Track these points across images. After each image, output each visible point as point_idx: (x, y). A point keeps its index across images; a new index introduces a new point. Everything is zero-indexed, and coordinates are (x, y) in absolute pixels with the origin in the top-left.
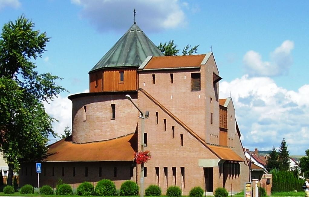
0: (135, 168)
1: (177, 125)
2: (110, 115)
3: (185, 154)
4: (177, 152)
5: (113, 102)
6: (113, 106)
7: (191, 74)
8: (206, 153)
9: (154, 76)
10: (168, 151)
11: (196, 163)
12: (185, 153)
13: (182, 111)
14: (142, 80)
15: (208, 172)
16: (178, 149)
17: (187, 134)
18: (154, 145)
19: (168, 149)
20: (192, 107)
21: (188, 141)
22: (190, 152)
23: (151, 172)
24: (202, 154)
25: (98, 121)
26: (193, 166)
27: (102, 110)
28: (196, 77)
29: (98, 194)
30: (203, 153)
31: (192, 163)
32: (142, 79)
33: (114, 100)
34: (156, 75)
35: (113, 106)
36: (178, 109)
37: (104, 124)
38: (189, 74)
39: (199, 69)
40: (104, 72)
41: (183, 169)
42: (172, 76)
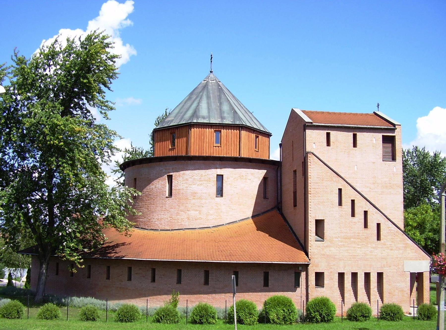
0: (303, 274)
1: (371, 210)
2: (213, 189)
3: (383, 252)
4: (372, 249)
5: (220, 171)
6: (220, 178)
7: (383, 136)
8: (414, 251)
9: (328, 135)
10: (358, 248)
11: (400, 266)
12: (384, 251)
13: (370, 188)
14: (312, 139)
15: (417, 278)
16: (374, 245)
17: (387, 223)
18: (336, 238)
19: (358, 245)
20: (386, 184)
21: (388, 233)
22: (392, 250)
23: (332, 279)
24: (409, 253)
25: (194, 199)
26: (395, 271)
27: (201, 182)
28: (389, 141)
29: (273, 320)
30: (410, 252)
31: (394, 265)
32: (311, 137)
33: (221, 168)
34: (333, 133)
35: (220, 178)
36: (366, 186)
37: (206, 203)
38: (379, 136)
39: (393, 130)
40: (192, 129)
41: (380, 275)
42: (355, 136)
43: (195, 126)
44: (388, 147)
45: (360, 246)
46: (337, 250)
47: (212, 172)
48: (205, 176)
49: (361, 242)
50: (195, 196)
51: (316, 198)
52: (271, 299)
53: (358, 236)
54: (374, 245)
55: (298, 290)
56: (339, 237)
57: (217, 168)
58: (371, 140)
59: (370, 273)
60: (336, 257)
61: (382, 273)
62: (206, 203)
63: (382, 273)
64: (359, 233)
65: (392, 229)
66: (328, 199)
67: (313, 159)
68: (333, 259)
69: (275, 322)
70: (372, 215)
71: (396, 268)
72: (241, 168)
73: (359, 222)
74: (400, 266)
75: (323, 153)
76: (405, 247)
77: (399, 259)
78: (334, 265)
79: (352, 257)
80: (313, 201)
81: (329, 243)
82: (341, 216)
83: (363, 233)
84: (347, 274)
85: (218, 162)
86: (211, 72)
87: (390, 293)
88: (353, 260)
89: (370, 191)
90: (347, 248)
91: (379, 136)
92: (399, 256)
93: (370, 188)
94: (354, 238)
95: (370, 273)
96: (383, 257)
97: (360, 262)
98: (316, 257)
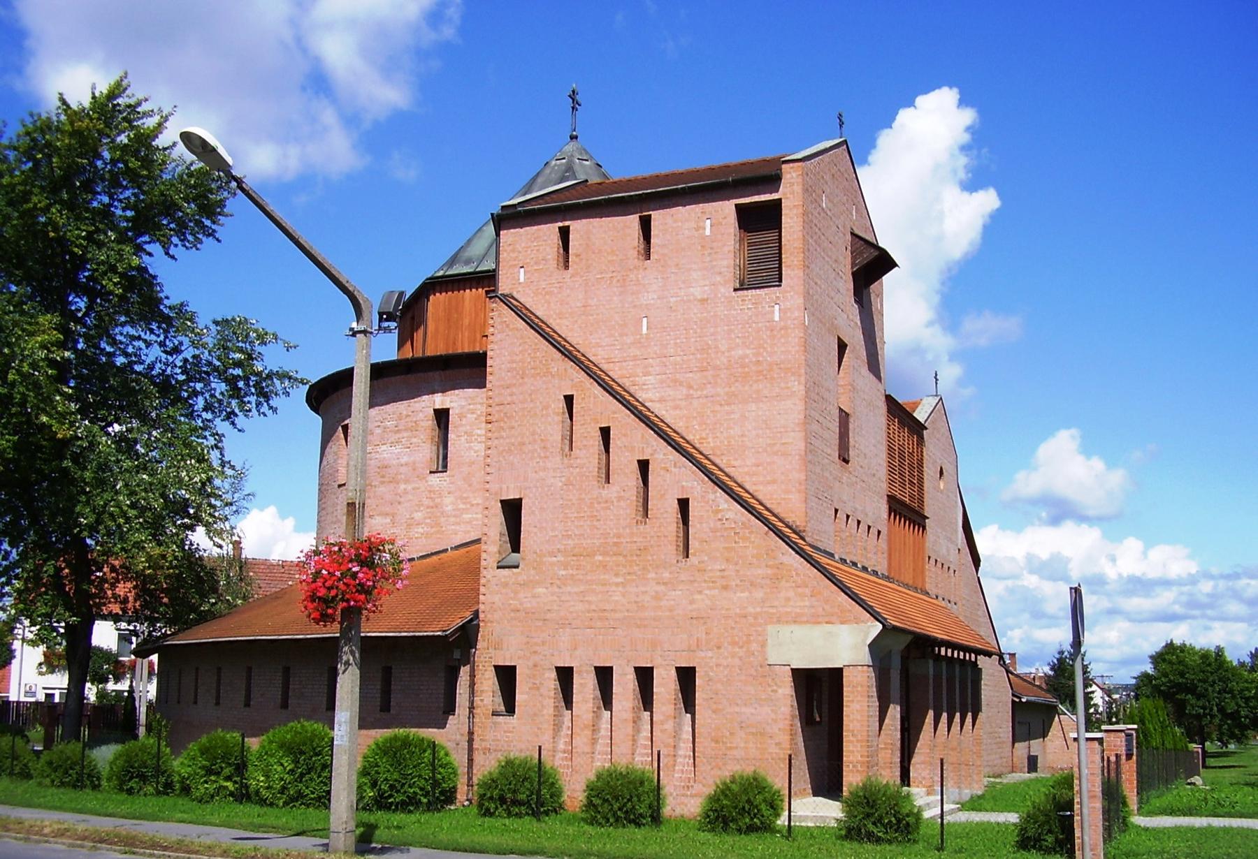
0: (464, 671)
1: (660, 454)
2: (426, 452)
3: (697, 597)
4: (662, 588)
5: (439, 400)
6: (442, 417)
7: (739, 207)
8: (807, 591)
9: (565, 233)
10: (617, 584)
11: (754, 646)
12: (700, 592)
13: (690, 387)
14: (513, 255)
15: (818, 691)
16: (666, 575)
17: (712, 496)
18: (552, 554)
19: (617, 575)
20: (743, 366)
21: (714, 531)
22: (725, 588)
23: (538, 689)
24: (788, 599)
25: (383, 483)
26: (737, 661)
27: (398, 436)
28: (760, 221)
29: (257, 792)
30: (791, 594)
31: (734, 643)
32: (513, 251)
33: (443, 391)
34: (578, 227)
35: (442, 417)
36: (675, 381)
37: (405, 492)
38: (726, 210)
39: (771, 179)
40: (431, 297)
41: (686, 677)
42: (646, 224)
43: (438, 288)
44: (768, 242)
45: (620, 580)
46: (552, 595)
47: (423, 404)
48: (407, 416)
49: (625, 566)
50: (383, 477)
51: (504, 434)
52: (733, 776)
53: (616, 544)
54: (666, 575)
55: (452, 720)
56: (559, 551)
57: (433, 393)
58: (697, 229)
59: (652, 669)
60: (548, 616)
61: (693, 669)
62: (405, 492)
63: (693, 669)
64: (619, 536)
65: (730, 515)
66: (533, 434)
67: (500, 316)
68: (540, 623)
69: (262, 802)
70: (662, 472)
71: (741, 652)
72: (333, 375)
73: (620, 498)
74: (754, 646)
75: (547, 293)
76: (776, 579)
77: (751, 620)
78: (544, 643)
79: (596, 615)
80: (496, 442)
81: (533, 572)
82: (568, 484)
83: (632, 534)
84: (580, 672)
85: (436, 375)
86: (573, 138)
87: (717, 742)
88: (599, 624)
89: (688, 397)
90: (582, 588)
91: (726, 210)
92: (751, 610)
93: (690, 387)
94: (605, 554)
95: (652, 669)
96: (694, 614)
97: (619, 632)
98: (497, 616)
